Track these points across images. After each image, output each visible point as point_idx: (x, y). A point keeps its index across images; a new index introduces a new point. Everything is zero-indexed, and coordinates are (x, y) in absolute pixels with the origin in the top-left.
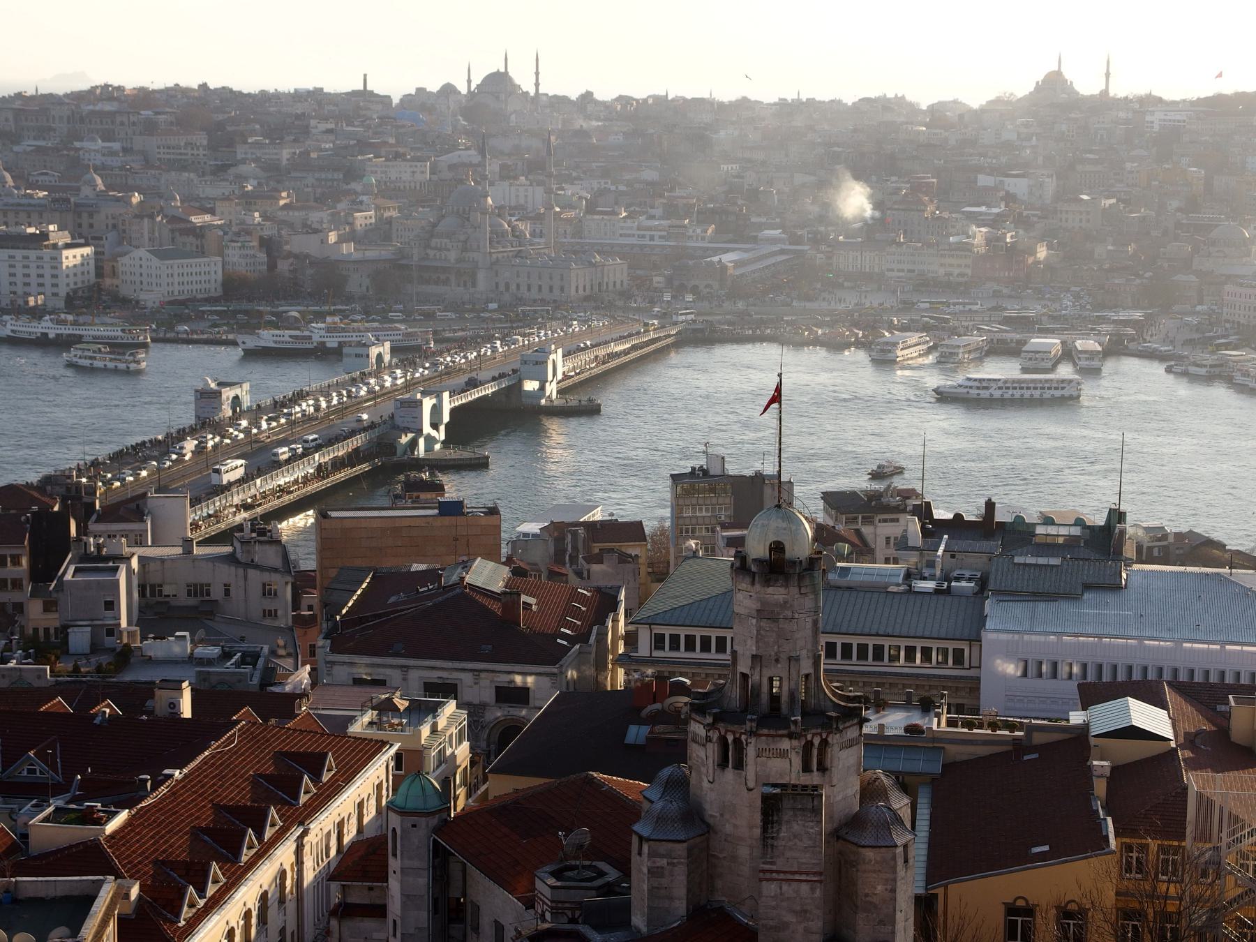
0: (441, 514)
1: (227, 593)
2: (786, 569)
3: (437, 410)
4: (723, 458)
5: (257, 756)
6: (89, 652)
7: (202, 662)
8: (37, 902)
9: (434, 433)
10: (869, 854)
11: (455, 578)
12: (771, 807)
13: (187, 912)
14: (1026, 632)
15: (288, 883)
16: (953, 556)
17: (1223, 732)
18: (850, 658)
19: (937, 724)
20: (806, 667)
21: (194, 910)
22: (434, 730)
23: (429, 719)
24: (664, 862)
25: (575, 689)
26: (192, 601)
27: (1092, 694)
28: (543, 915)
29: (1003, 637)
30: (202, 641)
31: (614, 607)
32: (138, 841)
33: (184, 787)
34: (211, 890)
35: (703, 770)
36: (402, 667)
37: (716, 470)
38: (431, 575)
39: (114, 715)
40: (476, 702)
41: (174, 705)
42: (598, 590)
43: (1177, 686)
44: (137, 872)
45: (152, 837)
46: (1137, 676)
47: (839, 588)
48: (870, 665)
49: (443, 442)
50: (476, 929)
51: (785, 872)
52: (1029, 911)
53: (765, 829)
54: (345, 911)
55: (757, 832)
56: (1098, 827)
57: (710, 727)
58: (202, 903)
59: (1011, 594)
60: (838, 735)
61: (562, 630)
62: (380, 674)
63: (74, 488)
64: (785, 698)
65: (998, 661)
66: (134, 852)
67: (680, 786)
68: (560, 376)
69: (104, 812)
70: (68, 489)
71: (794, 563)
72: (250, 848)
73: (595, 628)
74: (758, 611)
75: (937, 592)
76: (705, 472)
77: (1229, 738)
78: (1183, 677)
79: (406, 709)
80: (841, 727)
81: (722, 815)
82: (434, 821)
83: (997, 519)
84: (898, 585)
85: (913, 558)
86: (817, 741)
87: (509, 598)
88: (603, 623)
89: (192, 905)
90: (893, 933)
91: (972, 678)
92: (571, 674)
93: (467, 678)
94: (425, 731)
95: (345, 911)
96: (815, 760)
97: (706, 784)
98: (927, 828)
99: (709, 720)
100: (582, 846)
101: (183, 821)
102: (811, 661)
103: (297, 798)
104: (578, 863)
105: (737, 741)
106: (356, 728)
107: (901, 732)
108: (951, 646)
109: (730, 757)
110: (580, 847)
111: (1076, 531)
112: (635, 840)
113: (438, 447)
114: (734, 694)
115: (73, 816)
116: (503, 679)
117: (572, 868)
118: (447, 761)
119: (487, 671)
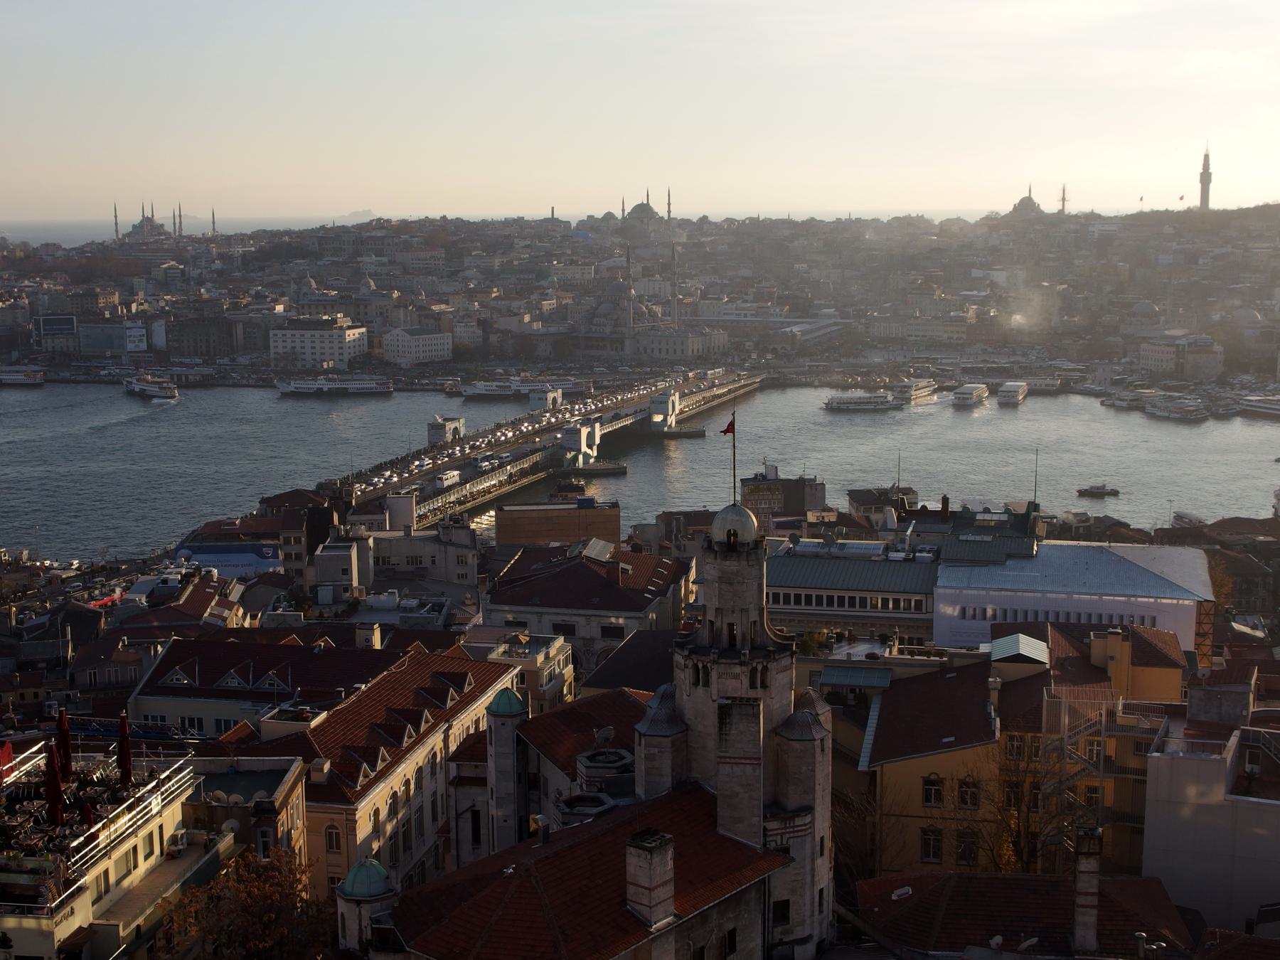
0: (579, 508)
1: (433, 562)
2: (738, 549)
3: (591, 436)
4: (776, 467)
5: (420, 675)
6: (331, 603)
7: (405, 609)
8: (251, 774)
9: (589, 451)
10: (796, 745)
11: (576, 552)
12: (724, 713)
13: (362, 781)
14: (966, 588)
15: (438, 759)
16: (918, 535)
17: (1085, 657)
18: (844, 606)
19: (892, 652)
20: (754, 616)
21: (367, 780)
22: (547, 657)
23: (544, 649)
24: (655, 750)
25: (657, 628)
26: (411, 568)
27: (1002, 629)
28: (581, 786)
29: (949, 591)
30: (406, 596)
31: (687, 570)
32: (332, 733)
33: (367, 696)
34: (380, 765)
35: (684, 687)
36: (537, 613)
37: (771, 476)
38: (561, 550)
39: (328, 649)
40: (588, 637)
41: (369, 640)
42: (677, 560)
43: (1057, 626)
44: (330, 754)
45: (343, 730)
46: (1031, 618)
47: (837, 558)
48: (857, 611)
49: (596, 457)
50: (546, 795)
51: (735, 758)
52: (940, 782)
53: (720, 728)
54: (459, 781)
55: (717, 729)
56: (988, 722)
57: (686, 658)
58: (373, 774)
59: (956, 562)
60: (775, 664)
61: (649, 587)
62: (522, 618)
63: (338, 491)
64: (739, 639)
65: (941, 605)
66: (329, 740)
67: (669, 697)
68: (677, 412)
69: (311, 713)
70: (334, 492)
71: (744, 544)
72: (410, 737)
73: (672, 586)
74: (720, 578)
75: (906, 560)
76: (764, 477)
77: (1090, 661)
78: (1062, 619)
79: (527, 642)
80: (777, 658)
81: (696, 718)
82: (517, 721)
83: (950, 510)
84: (879, 555)
85: (891, 537)
86: (760, 668)
87: (612, 565)
88: (677, 582)
89: (366, 776)
90: (814, 800)
91: (927, 620)
92: (653, 616)
93: (582, 621)
94: (540, 658)
95: (459, 781)
96: (759, 680)
97: (685, 696)
98: (875, 725)
99: (686, 653)
100: (608, 739)
101: (365, 719)
102: (757, 612)
103: (445, 704)
104: (605, 750)
105: (705, 667)
106: (493, 656)
107: (864, 658)
108: (914, 598)
109: (701, 678)
110: (608, 739)
111: (1004, 517)
112: (637, 735)
113: (592, 461)
114: (704, 636)
115: (290, 715)
116: (605, 621)
117: (602, 754)
118: (557, 679)
119: (595, 616)
